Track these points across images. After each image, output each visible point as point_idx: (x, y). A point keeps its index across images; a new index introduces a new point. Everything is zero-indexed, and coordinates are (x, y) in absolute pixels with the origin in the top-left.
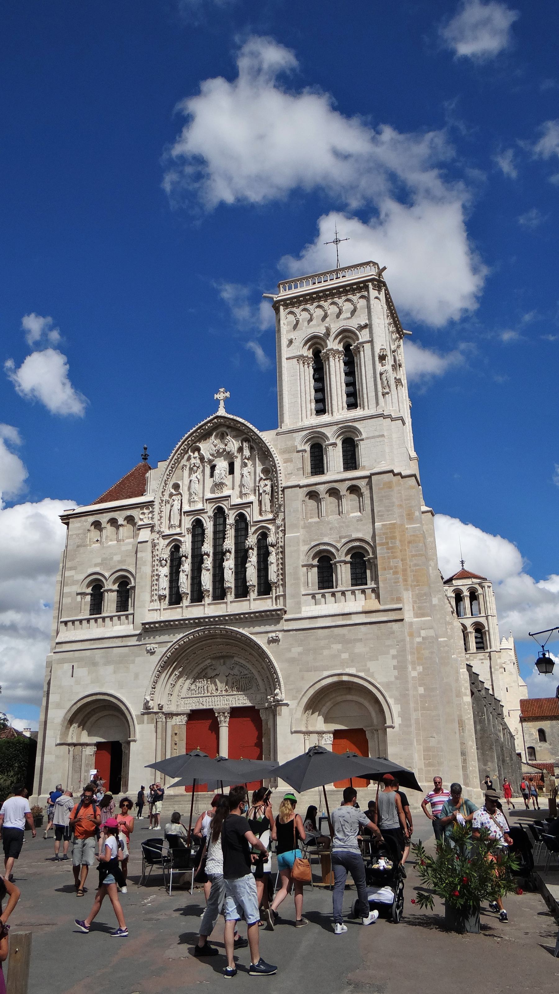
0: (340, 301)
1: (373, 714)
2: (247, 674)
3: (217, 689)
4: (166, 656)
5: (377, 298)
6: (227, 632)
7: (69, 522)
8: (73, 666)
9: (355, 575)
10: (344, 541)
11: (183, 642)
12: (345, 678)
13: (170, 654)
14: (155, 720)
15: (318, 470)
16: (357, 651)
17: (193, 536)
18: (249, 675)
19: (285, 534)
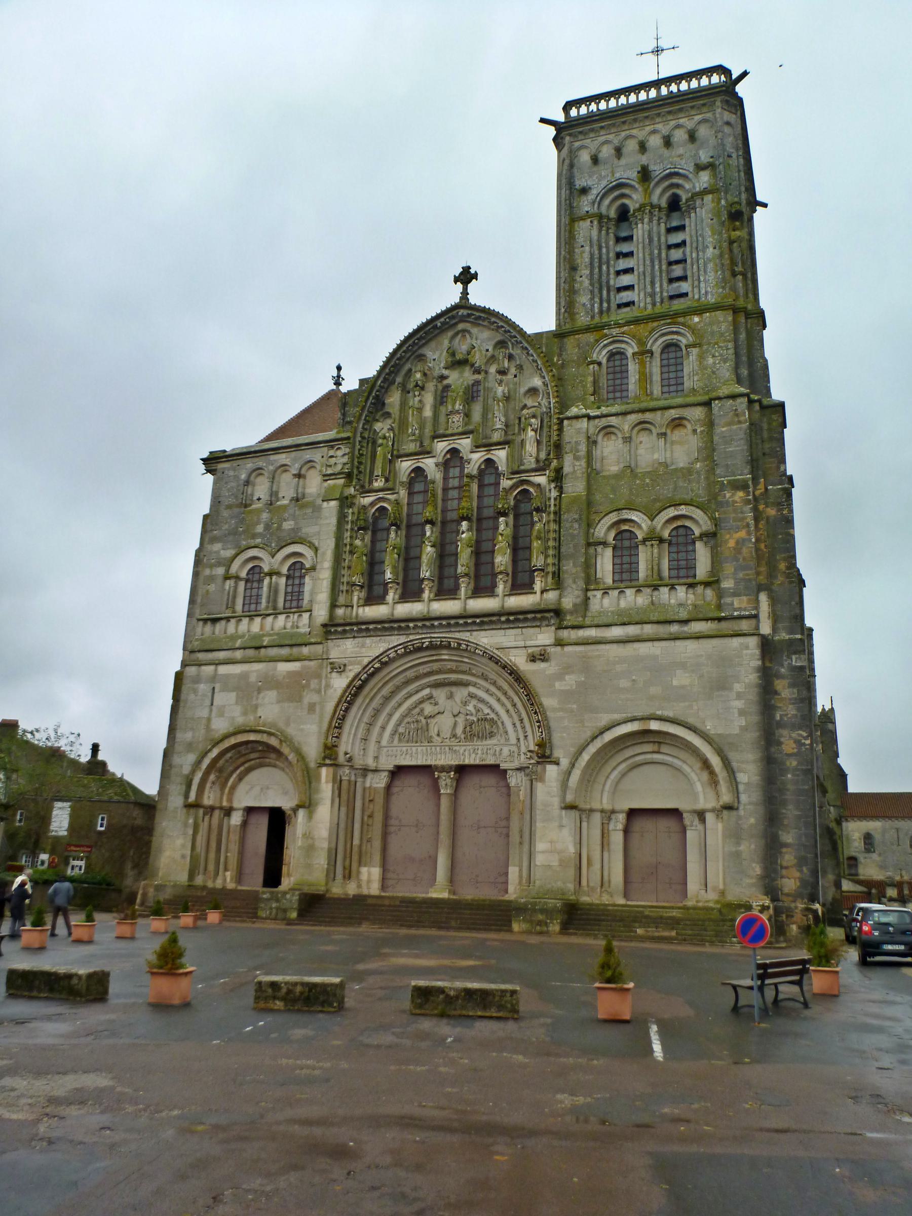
0: (664, 128)
1: (699, 787)
2: (488, 714)
3: (438, 735)
4: (360, 679)
5: (728, 123)
6: (459, 645)
7: (215, 470)
8: (214, 688)
9: (676, 563)
10: (658, 505)
11: (386, 659)
12: (654, 726)
13: (365, 675)
14: (339, 777)
15: (618, 395)
16: (675, 683)
17: (411, 494)
18: (492, 716)
19: (561, 493)
